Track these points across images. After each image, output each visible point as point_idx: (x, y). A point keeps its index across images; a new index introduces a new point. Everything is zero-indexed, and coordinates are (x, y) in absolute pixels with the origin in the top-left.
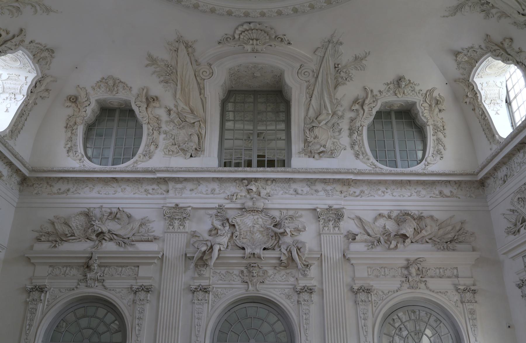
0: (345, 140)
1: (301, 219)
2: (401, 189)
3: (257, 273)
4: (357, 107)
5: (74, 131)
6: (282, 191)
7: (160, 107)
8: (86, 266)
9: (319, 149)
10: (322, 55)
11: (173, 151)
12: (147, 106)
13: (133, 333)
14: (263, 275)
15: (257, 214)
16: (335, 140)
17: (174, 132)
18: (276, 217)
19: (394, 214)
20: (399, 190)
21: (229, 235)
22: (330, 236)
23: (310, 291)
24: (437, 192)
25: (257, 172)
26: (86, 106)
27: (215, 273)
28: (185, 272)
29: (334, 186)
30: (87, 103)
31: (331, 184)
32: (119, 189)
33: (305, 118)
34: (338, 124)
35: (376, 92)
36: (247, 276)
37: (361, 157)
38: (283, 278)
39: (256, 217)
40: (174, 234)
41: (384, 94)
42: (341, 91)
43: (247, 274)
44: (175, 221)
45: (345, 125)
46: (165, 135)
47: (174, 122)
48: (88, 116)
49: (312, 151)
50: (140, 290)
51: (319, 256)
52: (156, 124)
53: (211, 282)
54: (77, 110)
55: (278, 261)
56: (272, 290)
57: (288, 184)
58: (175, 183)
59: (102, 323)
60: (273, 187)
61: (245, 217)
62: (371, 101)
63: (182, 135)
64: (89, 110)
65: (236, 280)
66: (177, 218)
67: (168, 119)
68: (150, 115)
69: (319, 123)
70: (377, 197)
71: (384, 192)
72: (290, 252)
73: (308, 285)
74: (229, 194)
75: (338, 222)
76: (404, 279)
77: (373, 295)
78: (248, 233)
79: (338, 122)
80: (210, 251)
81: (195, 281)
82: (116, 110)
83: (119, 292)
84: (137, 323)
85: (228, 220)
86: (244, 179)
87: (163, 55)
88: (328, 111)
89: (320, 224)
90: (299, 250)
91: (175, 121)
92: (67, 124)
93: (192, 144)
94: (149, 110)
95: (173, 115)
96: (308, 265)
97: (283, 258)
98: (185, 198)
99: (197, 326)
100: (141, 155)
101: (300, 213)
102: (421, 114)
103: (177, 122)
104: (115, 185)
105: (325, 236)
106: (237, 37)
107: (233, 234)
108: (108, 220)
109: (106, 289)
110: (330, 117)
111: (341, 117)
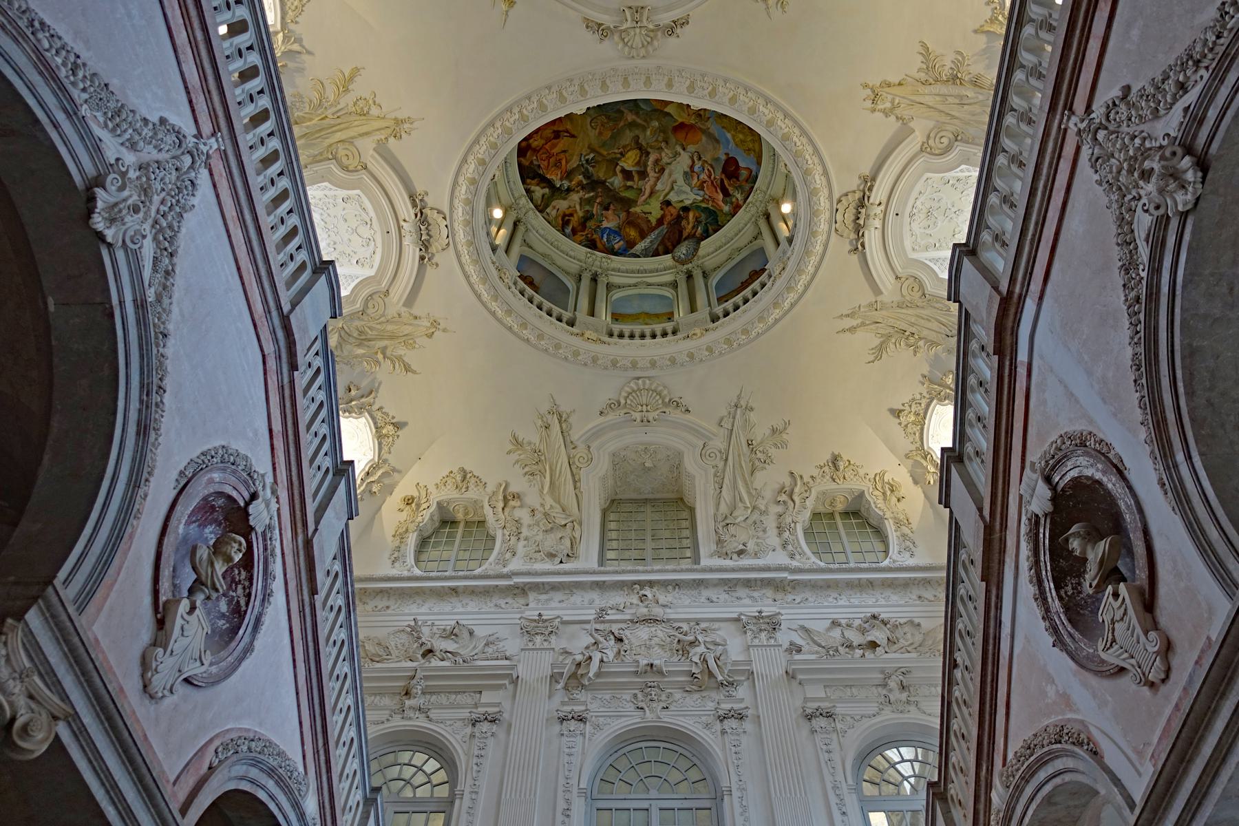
4: (784, 497)
7: (521, 506)
10: (730, 428)
13: (469, 772)
24: (914, 597)
27: (595, 698)
29: (764, 591)
32: (459, 605)
35: (806, 479)
37: (798, 557)
39: (653, 629)
41: (818, 480)
42: (760, 478)
45: (770, 523)
52: (514, 529)
60: (677, 595)
62: (803, 490)
63: (550, 542)
64: (427, 515)
72: (705, 661)
78: (643, 648)
84: (475, 761)
86: (635, 583)
87: (531, 435)
93: (562, 547)
94: (507, 510)
95: (538, 516)
97: (694, 670)
101: (716, 625)
102: (873, 505)
106: (623, 402)
110: (749, 511)
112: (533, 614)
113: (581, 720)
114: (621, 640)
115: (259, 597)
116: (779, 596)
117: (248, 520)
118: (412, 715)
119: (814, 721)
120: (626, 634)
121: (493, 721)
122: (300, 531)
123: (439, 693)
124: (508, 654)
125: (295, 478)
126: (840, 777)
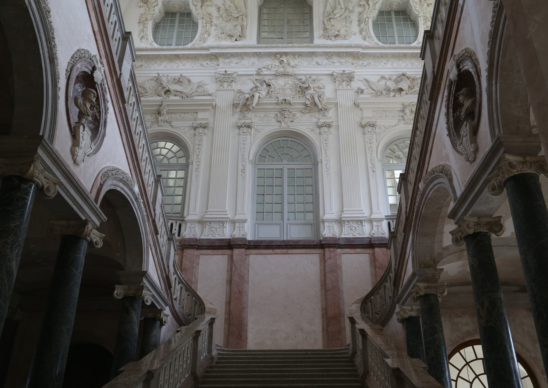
0: (355, 28)
1: (322, 82)
2: (399, 62)
5: (145, 25)
7: (211, 6)
8: (157, 113)
9: (334, 33)
11: (222, 38)
12: (202, 5)
13: (195, 153)
14: (292, 117)
16: (347, 29)
17: (222, 25)
19: (394, 77)
20: (397, 62)
22: (344, 91)
23: (329, 126)
25: (287, 47)
26: (155, 6)
28: (233, 116)
29: (347, 59)
30: (155, 4)
32: (181, 65)
33: (324, 12)
34: (349, 17)
37: (367, 39)
39: (286, 80)
40: (224, 92)
45: (354, 17)
46: (216, 27)
47: (222, 17)
48: (156, 14)
49: (330, 35)
50: (199, 127)
52: (208, 19)
54: (148, 9)
56: (300, 127)
57: (311, 58)
58: (224, 59)
59: (170, 152)
60: (300, 60)
61: (278, 80)
63: (229, 27)
64: (157, 9)
65: (272, 121)
67: (218, 15)
68: (204, 12)
69: (335, 16)
70: (380, 66)
71: (385, 64)
72: (313, 98)
76: (401, 118)
77: (377, 128)
78: (281, 90)
79: (350, 15)
80: (252, 98)
82: (176, 13)
83: (183, 129)
84: (197, 147)
86: (277, 53)
88: (341, 6)
90: (320, 97)
91: (224, 16)
92: (140, 20)
93: (237, 31)
94: (204, 8)
95: (222, 11)
97: (308, 102)
99: (242, 149)
100: (197, 40)
101: (320, 77)
103: (225, 17)
104: (178, 62)
108: (173, 84)
109: (173, 127)
110: (343, 10)
111: (351, 12)
112: (221, 70)
113: (249, 127)
114: (269, 85)
115: (104, 111)
116: (355, 61)
117: (94, 80)
118: (163, 124)
119: (365, 128)
120: (273, 82)
121: (205, 127)
122: (114, 76)
123: (175, 113)
124: (210, 92)
125: (108, 52)
126: (374, 155)
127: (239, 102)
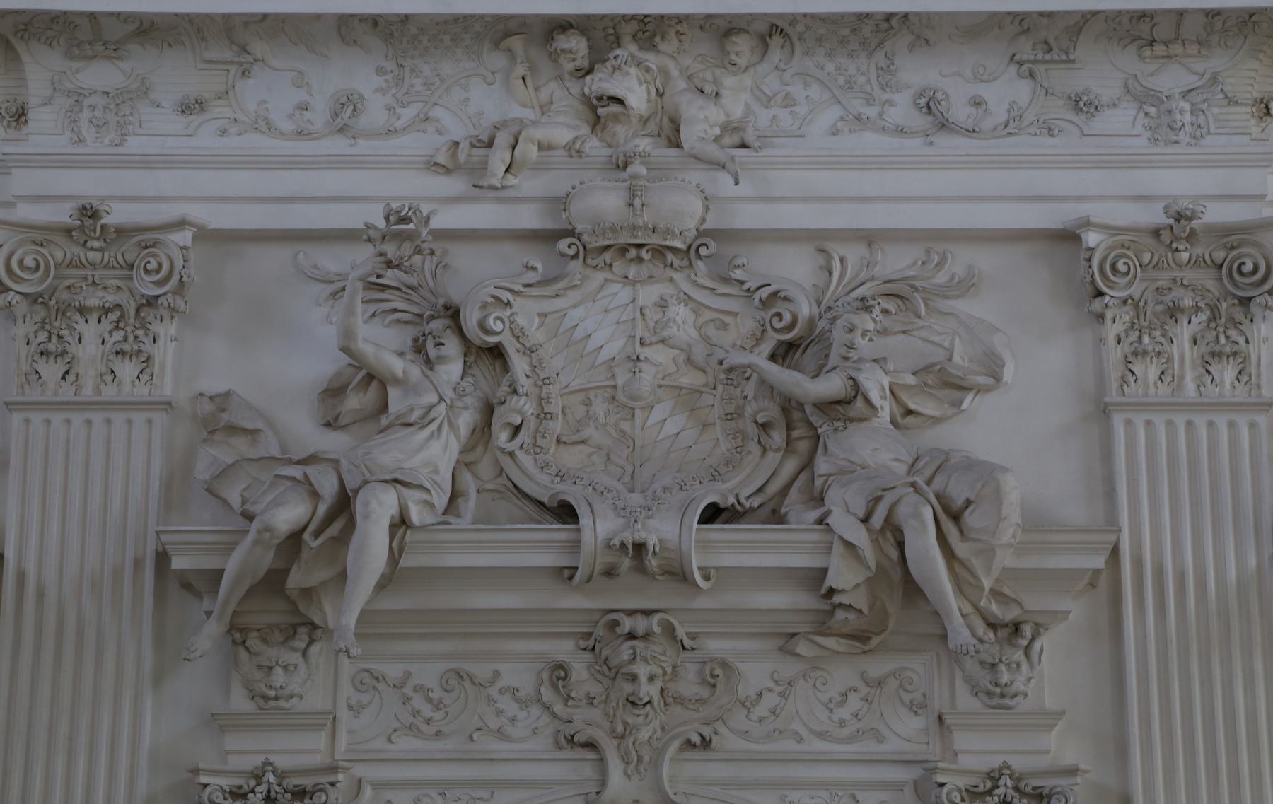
3: (659, 684)
6: (834, 112)
14: (704, 692)
15: (658, 270)
18: (792, 292)
21: (466, 420)
22: (1180, 420)
27: (369, 681)
28: (159, 679)
29: (1216, 62)
31: (1193, 49)
36: (591, 700)
38: (844, 713)
39: (649, 294)
40: (78, 418)
43: (595, 689)
44: (81, 326)
51: (1099, 562)
53: (343, 741)
55: (805, 600)
57: (879, 57)
58: (69, 56)
60: (771, 84)
61: (573, 296)
66: (93, 302)
72: (894, 532)
73: (1019, 763)
74: (458, 130)
75: (1236, 324)
78: (599, 408)
81: (233, 741)
85: (453, 314)
89: (1101, 340)
90: (956, 517)
96: (1016, 628)
97: (843, 575)
98: (146, 163)
101: (962, 259)
105: (1139, 420)
107: (489, 410)
127: (210, 563)
